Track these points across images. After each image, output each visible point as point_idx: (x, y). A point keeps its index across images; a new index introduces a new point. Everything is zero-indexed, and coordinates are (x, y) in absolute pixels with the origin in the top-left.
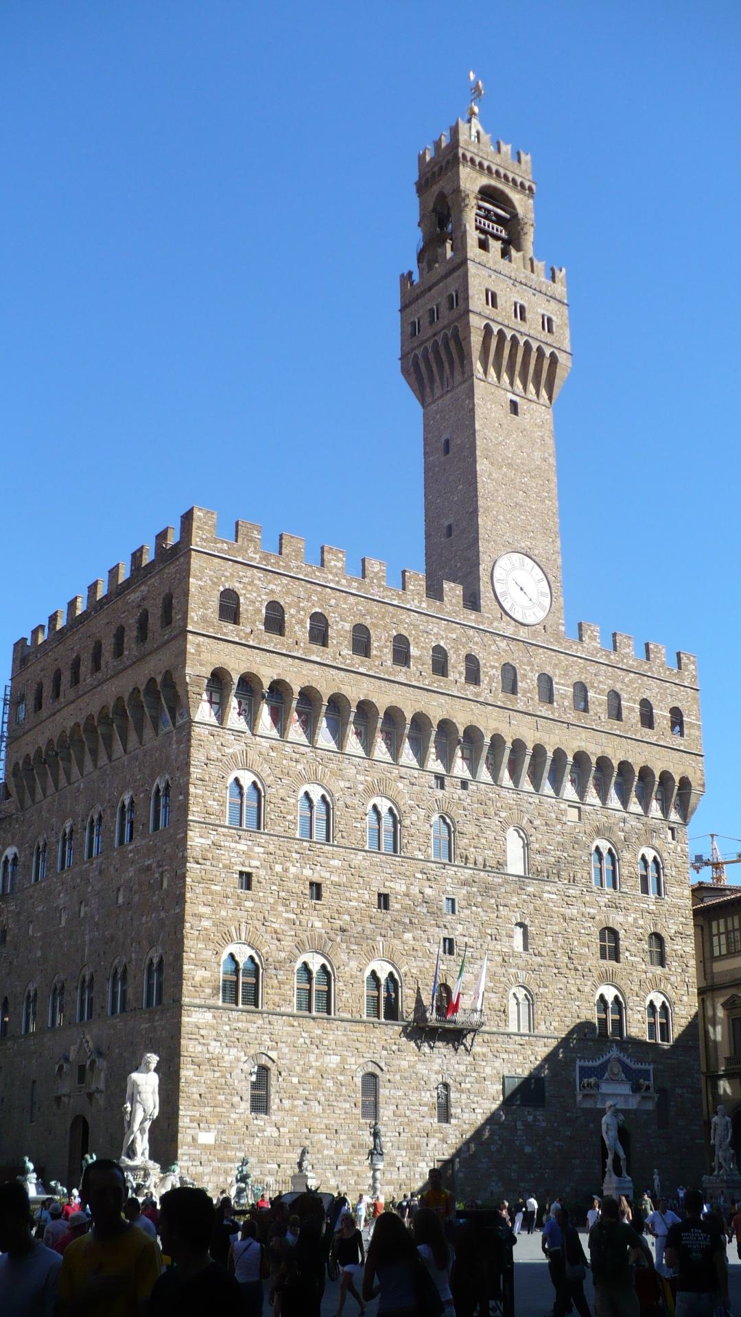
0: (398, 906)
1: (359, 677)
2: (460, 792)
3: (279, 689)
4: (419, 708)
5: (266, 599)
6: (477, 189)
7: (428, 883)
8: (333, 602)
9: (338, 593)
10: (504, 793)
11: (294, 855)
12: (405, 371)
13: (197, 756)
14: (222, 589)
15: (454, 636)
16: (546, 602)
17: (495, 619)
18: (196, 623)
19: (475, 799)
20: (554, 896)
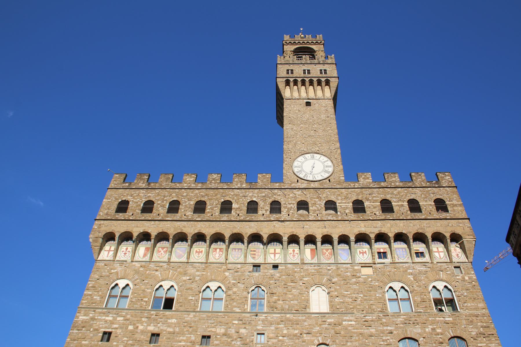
0: (216, 342)
1: (196, 223)
2: (272, 271)
3: (145, 237)
4: (235, 231)
5: (144, 200)
6: (292, 49)
7: (244, 326)
8: (185, 194)
9: (189, 190)
10: (306, 267)
11: (143, 319)
12: (278, 122)
13: (94, 276)
14: (120, 200)
15: (264, 195)
16: (331, 170)
17: (294, 182)
18: (102, 216)
19: (283, 273)
20: (353, 323)
